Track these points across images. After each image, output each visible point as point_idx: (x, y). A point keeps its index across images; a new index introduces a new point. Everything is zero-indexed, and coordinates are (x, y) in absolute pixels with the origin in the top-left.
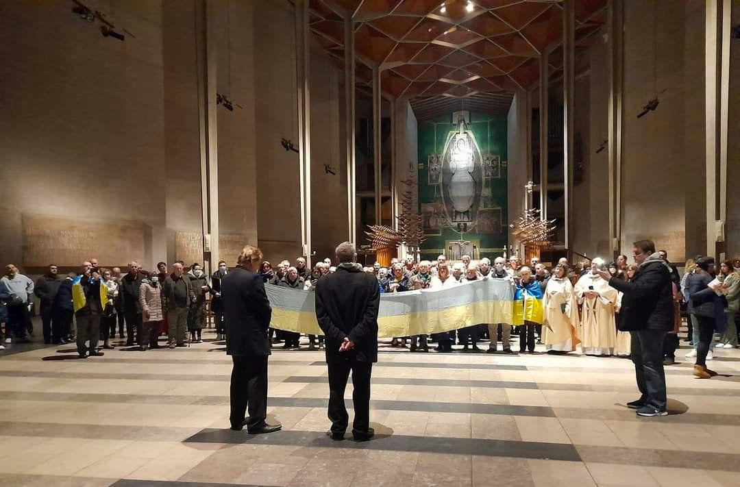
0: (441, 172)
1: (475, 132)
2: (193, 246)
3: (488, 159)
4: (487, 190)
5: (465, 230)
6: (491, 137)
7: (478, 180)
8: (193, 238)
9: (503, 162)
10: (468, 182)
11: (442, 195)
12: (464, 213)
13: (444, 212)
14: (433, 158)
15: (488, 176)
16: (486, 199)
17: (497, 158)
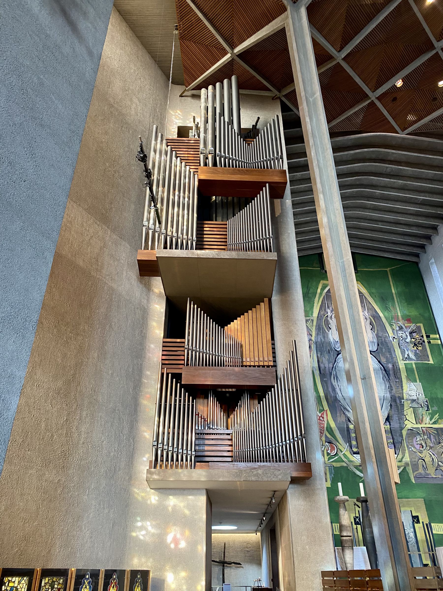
3: (401, 328)
6: (399, 294)
7: (390, 366)
9: (432, 336)
17: (419, 328)
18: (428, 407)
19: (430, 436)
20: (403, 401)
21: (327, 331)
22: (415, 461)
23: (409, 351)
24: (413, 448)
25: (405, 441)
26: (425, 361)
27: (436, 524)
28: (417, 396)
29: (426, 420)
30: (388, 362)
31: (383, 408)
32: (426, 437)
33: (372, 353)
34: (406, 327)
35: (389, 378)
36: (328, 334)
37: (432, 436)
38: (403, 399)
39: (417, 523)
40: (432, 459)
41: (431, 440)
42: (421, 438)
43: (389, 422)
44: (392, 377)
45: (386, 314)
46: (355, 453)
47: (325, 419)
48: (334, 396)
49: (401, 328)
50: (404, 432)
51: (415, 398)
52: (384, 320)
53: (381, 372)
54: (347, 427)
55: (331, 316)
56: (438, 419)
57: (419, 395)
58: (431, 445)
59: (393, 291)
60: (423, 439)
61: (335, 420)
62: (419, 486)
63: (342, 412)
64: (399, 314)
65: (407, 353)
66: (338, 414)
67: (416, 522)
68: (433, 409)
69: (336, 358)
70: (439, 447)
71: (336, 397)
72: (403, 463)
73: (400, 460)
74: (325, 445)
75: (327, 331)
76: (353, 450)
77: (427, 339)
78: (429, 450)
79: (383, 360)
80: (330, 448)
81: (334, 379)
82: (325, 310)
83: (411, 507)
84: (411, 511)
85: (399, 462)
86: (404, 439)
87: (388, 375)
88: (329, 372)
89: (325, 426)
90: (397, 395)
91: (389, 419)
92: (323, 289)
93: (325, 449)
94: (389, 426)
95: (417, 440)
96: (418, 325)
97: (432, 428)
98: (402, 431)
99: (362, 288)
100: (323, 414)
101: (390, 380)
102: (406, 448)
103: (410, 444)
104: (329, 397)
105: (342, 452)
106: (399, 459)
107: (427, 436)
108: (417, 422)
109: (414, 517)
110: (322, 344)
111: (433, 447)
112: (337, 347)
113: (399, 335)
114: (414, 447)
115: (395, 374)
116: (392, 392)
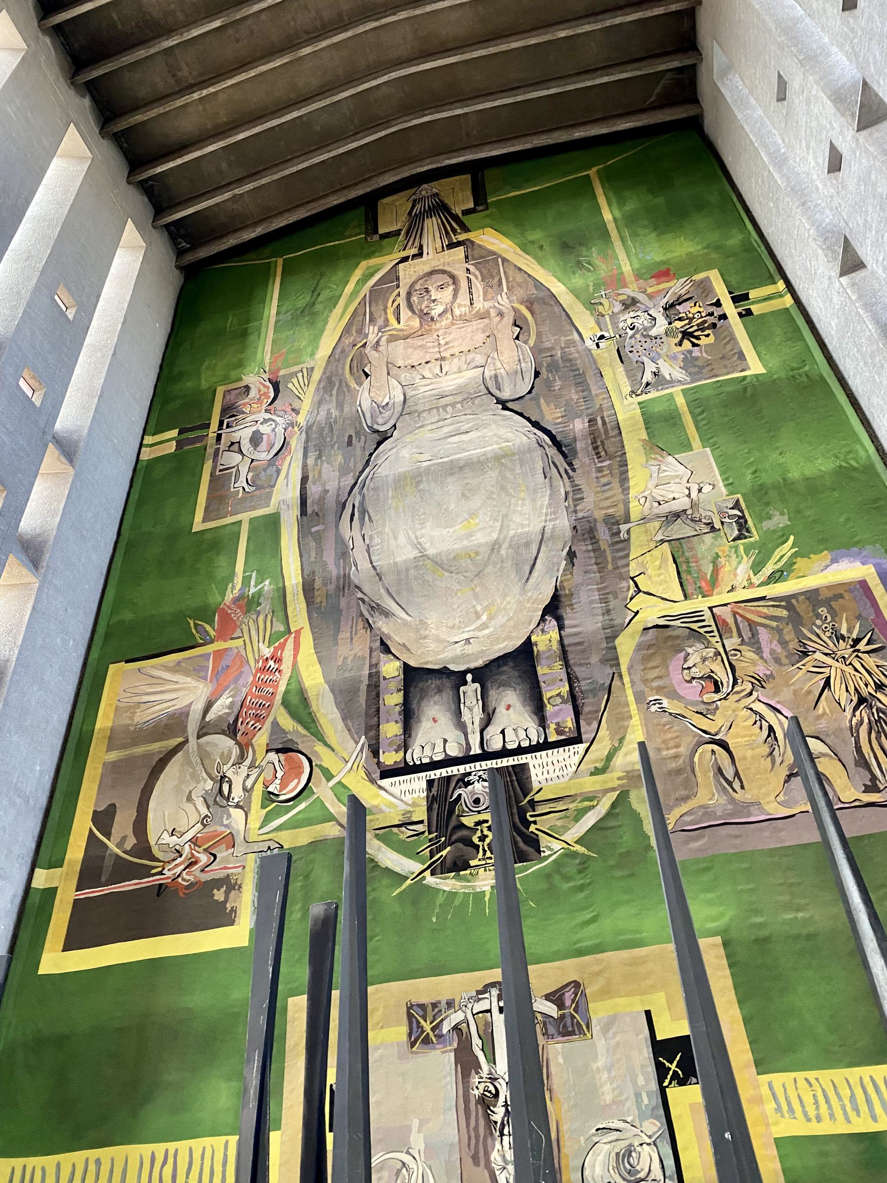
0: (296, 443)
4: (672, 466)
7: (579, 426)
11: (293, 575)
16: (681, 530)
18: (742, 524)
19: (754, 635)
20: (624, 528)
21: (353, 385)
22: (676, 757)
23: (660, 362)
24: (665, 703)
25: (626, 679)
26: (728, 373)
27: (800, 1075)
28: (689, 496)
29: (735, 575)
30: (570, 414)
31: (535, 574)
32: (732, 642)
33: (509, 405)
34: (650, 297)
35: (570, 464)
36: (354, 394)
37: (764, 635)
38: (627, 520)
39: (682, 1082)
40: (765, 732)
41: (759, 651)
42: (711, 652)
43: (559, 620)
45: (578, 280)
46: (387, 773)
47: (286, 666)
48: (338, 578)
49: (630, 304)
50: (626, 645)
51: (682, 503)
53: (539, 451)
54: (370, 675)
55: (378, 342)
56: (795, 555)
57: (700, 490)
58: (761, 670)
59: (607, 216)
60: (718, 654)
63: (361, 624)
65: (650, 367)
66: (344, 635)
67: (675, 1074)
68: (767, 525)
69: (371, 455)
70: (801, 673)
71: (346, 577)
72: (613, 778)
73: (599, 765)
74: (264, 764)
75: (353, 385)
76: (382, 760)
77: (736, 307)
78: (751, 694)
79: (551, 416)
80: (280, 774)
81: (352, 520)
82: (360, 331)
83: (652, 989)
84: (648, 1014)
85: (597, 772)
86: (624, 668)
87: (565, 456)
88: (337, 502)
89: (282, 688)
90: (599, 515)
91: (557, 608)
93: (261, 779)
94: (554, 635)
95: (689, 663)
96: (698, 277)
97: (763, 598)
98: (617, 642)
99: (496, 241)
100: (282, 647)
101: (574, 470)
102: (633, 707)
103: (654, 684)
104: (318, 584)
105: (329, 776)
106: (596, 761)
107: (740, 635)
108: (690, 589)
111: (771, 676)
112: (380, 420)
113: (621, 325)
114: (673, 695)
115: (596, 448)
116: (578, 508)
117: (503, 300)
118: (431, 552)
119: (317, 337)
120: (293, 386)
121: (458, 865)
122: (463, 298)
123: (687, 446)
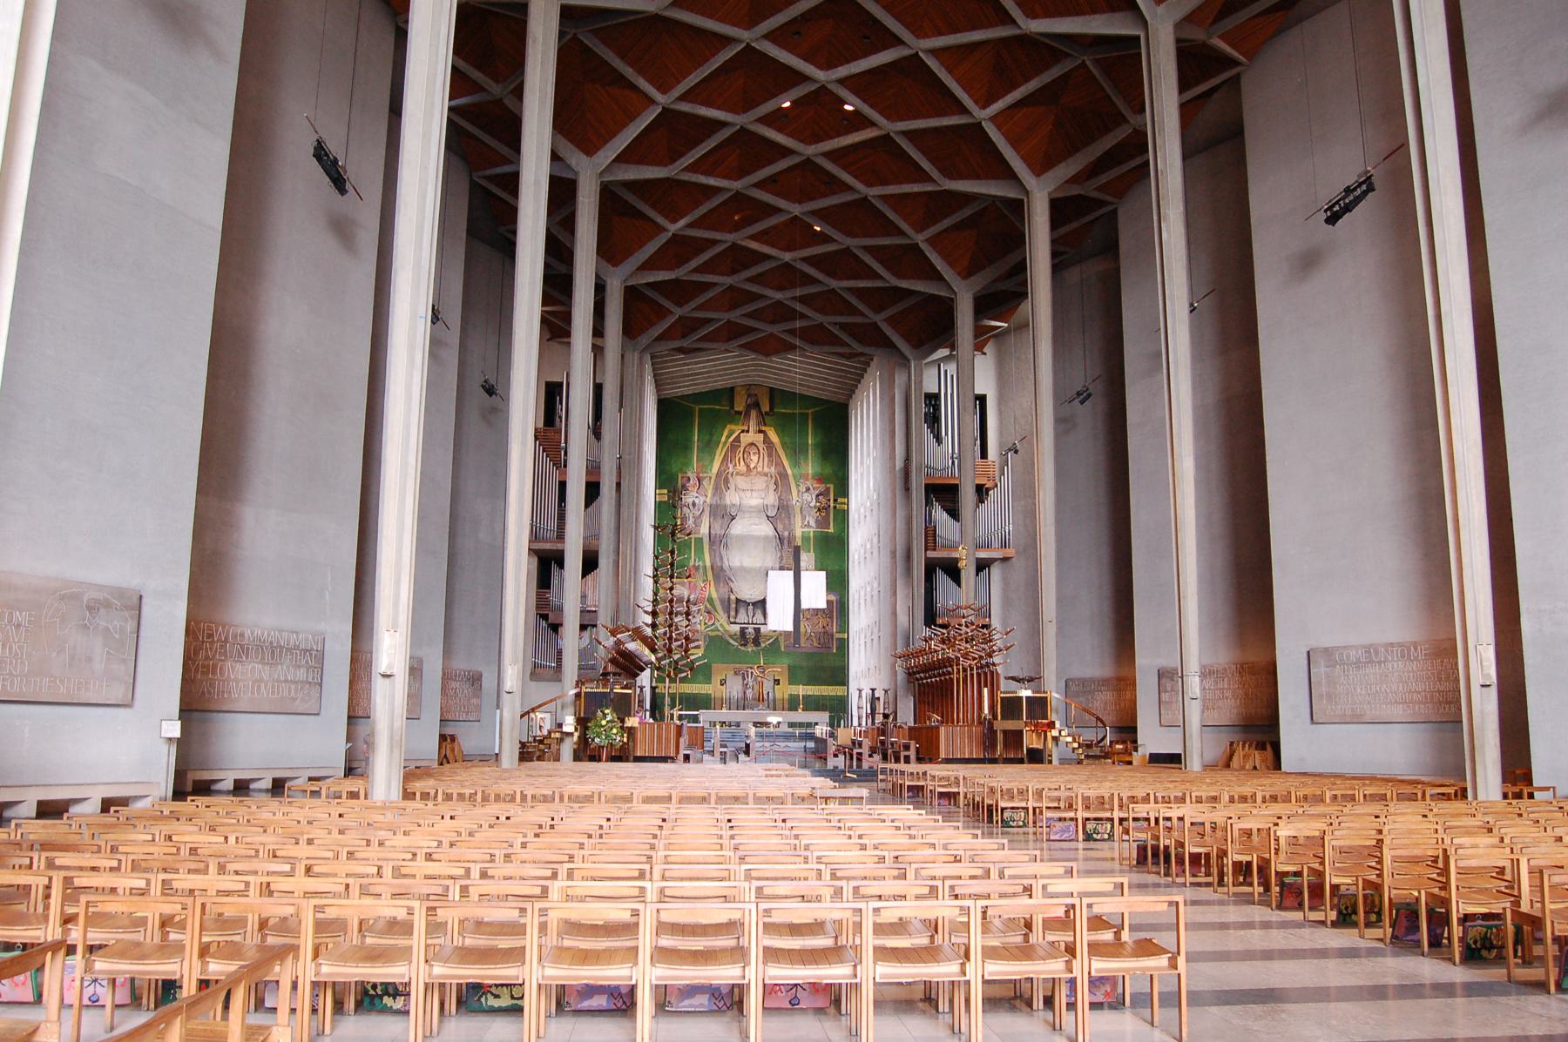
1: (781, 432)
2: (207, 658)
3: (808, 490)
5: (756, 642)
6: (816, 446)
7: (786, 534)
8: (210, 636)
9: (839, 500)
10: (766, 538)
11: (708, 564)
12: (754, 604)
13: (710, 600)
14: (689, 479)
15: (808, 525)
17: (828, 490)
30: (785, 529)
44: (786, 547)
45: (795, 471)
49: (808, 490)
52: (791, 479)
61: (717, 591)
62: (788, 654)
64: (810, 472)
71: (722, 567)
79: (780, 527)
92: (728, 437)
109: (775, 680)
110: (717, 506)
117: (773, 469)
118: (745, 565)
119: (712, 461)
120: (705, 483)
121: (745, 645)
122: (761, 463)
123: (809, 551)
